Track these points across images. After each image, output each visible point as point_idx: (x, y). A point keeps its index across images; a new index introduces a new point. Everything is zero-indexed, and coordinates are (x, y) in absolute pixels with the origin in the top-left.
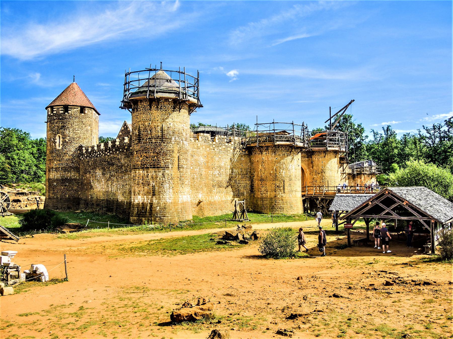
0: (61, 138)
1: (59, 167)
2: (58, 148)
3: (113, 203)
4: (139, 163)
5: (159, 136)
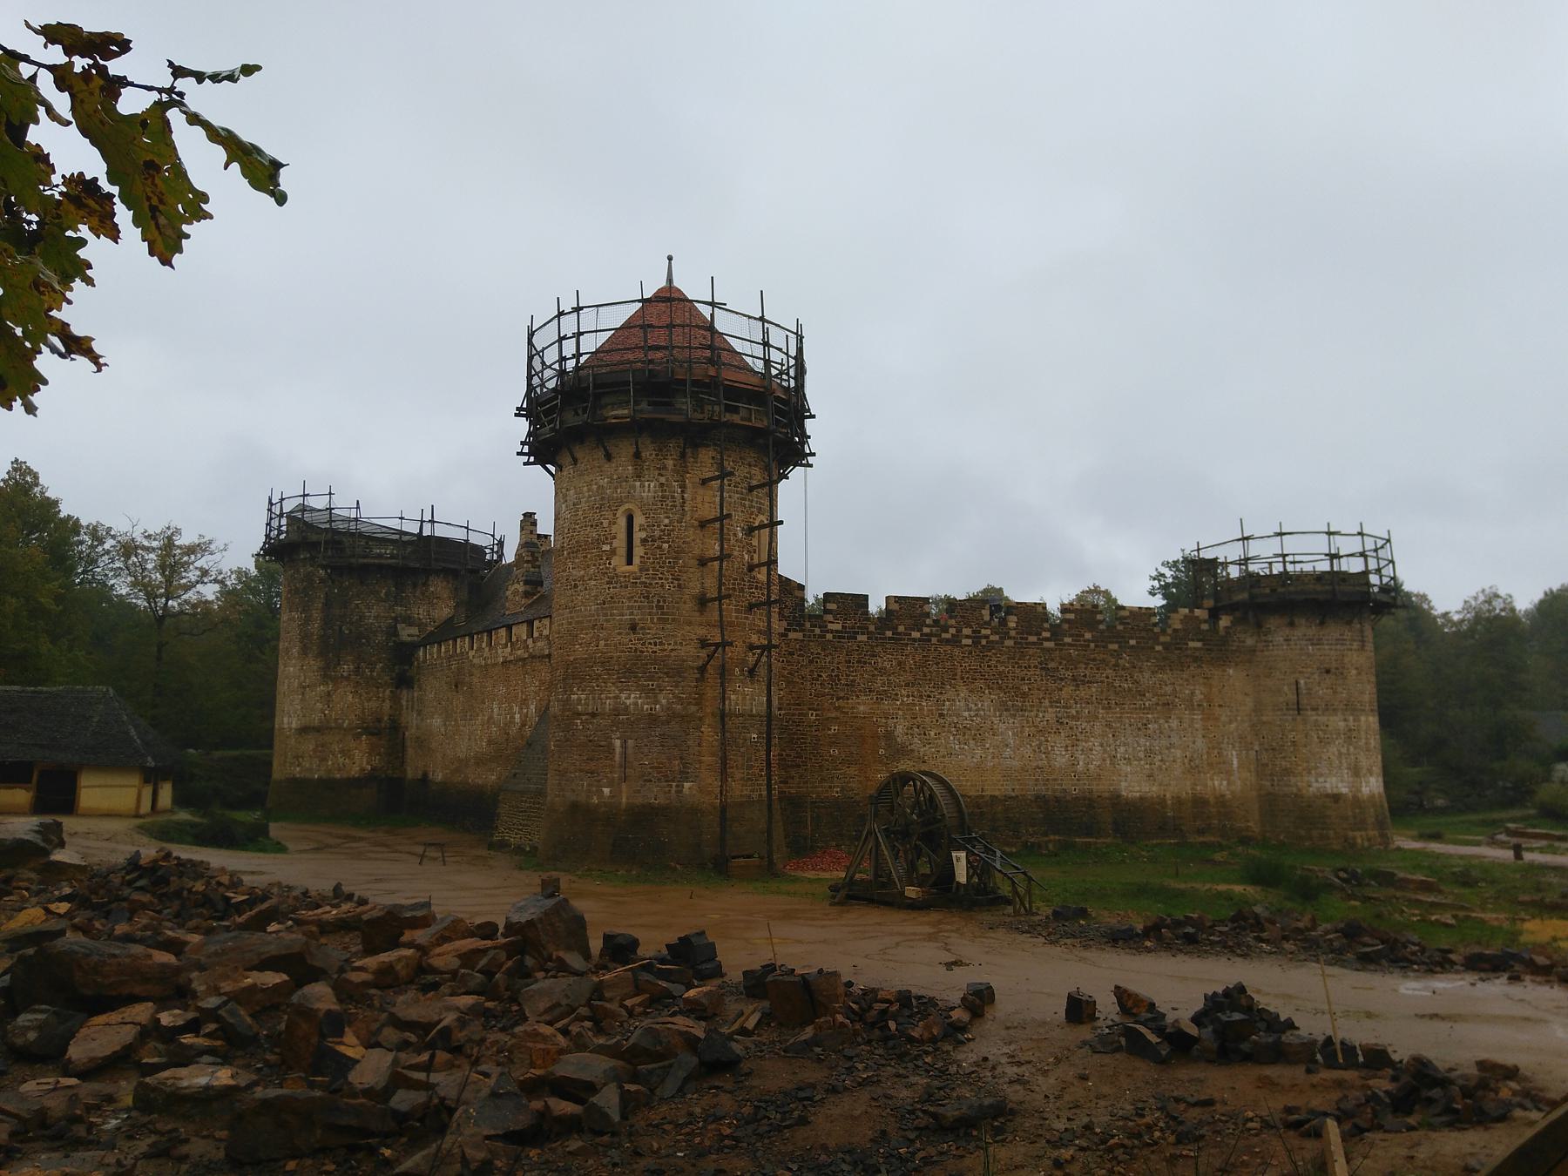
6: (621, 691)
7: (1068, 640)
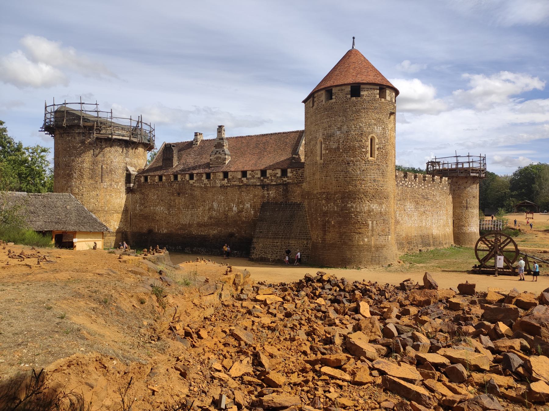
6: (371, 204)
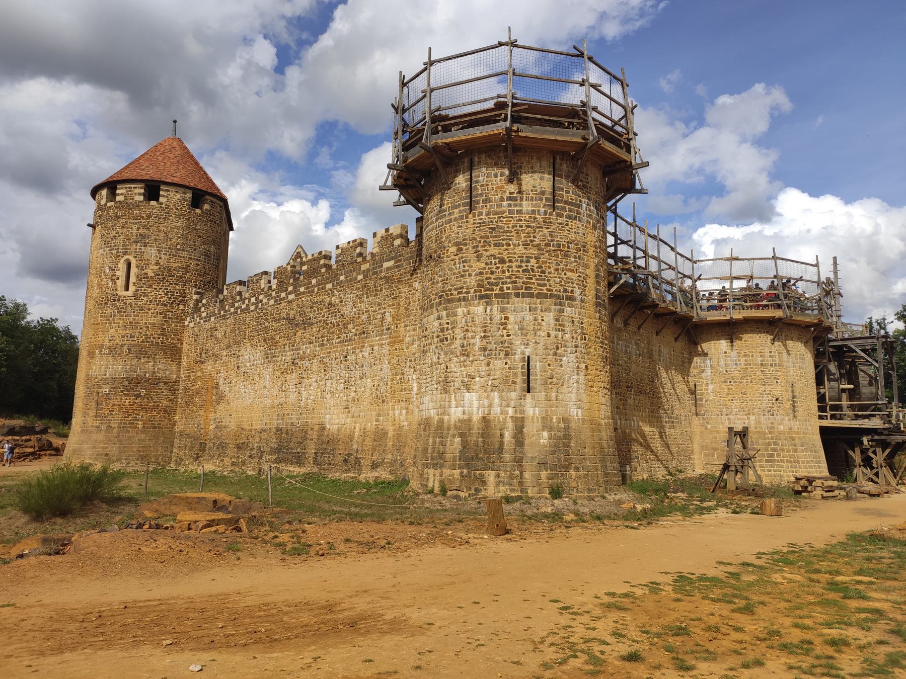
0: (133, 266)
1: (122, 345)
2: (122, 293)
3: (304, 438)
4: (472, 281)
5: (543, 193)
7: (302, 289)
